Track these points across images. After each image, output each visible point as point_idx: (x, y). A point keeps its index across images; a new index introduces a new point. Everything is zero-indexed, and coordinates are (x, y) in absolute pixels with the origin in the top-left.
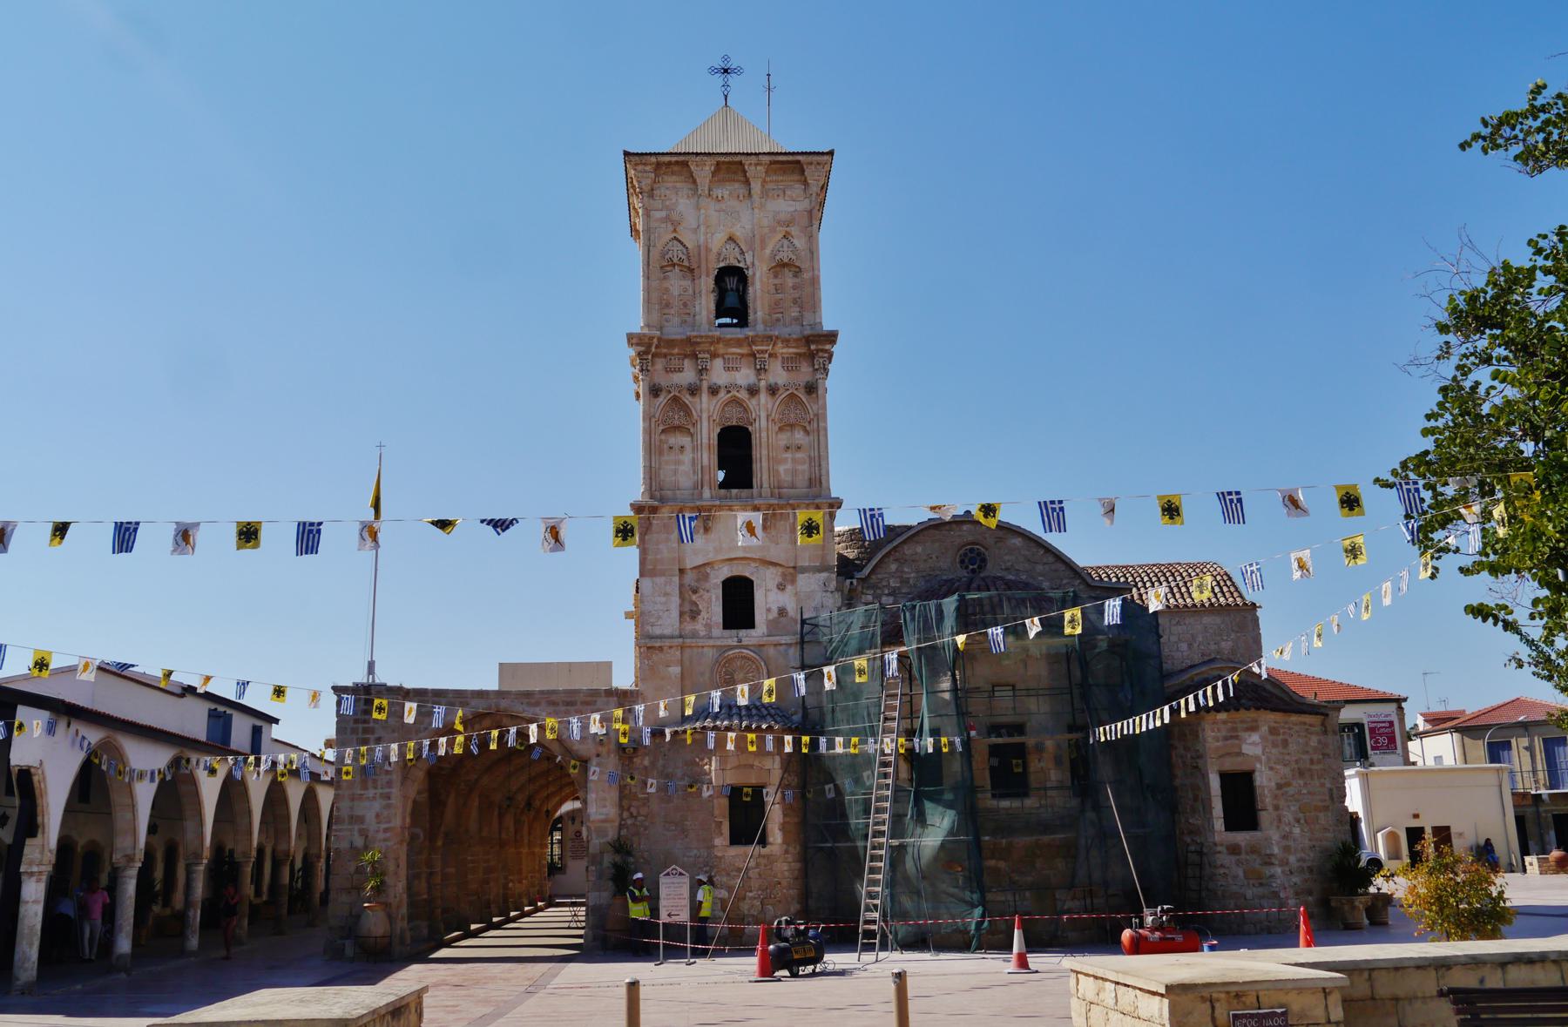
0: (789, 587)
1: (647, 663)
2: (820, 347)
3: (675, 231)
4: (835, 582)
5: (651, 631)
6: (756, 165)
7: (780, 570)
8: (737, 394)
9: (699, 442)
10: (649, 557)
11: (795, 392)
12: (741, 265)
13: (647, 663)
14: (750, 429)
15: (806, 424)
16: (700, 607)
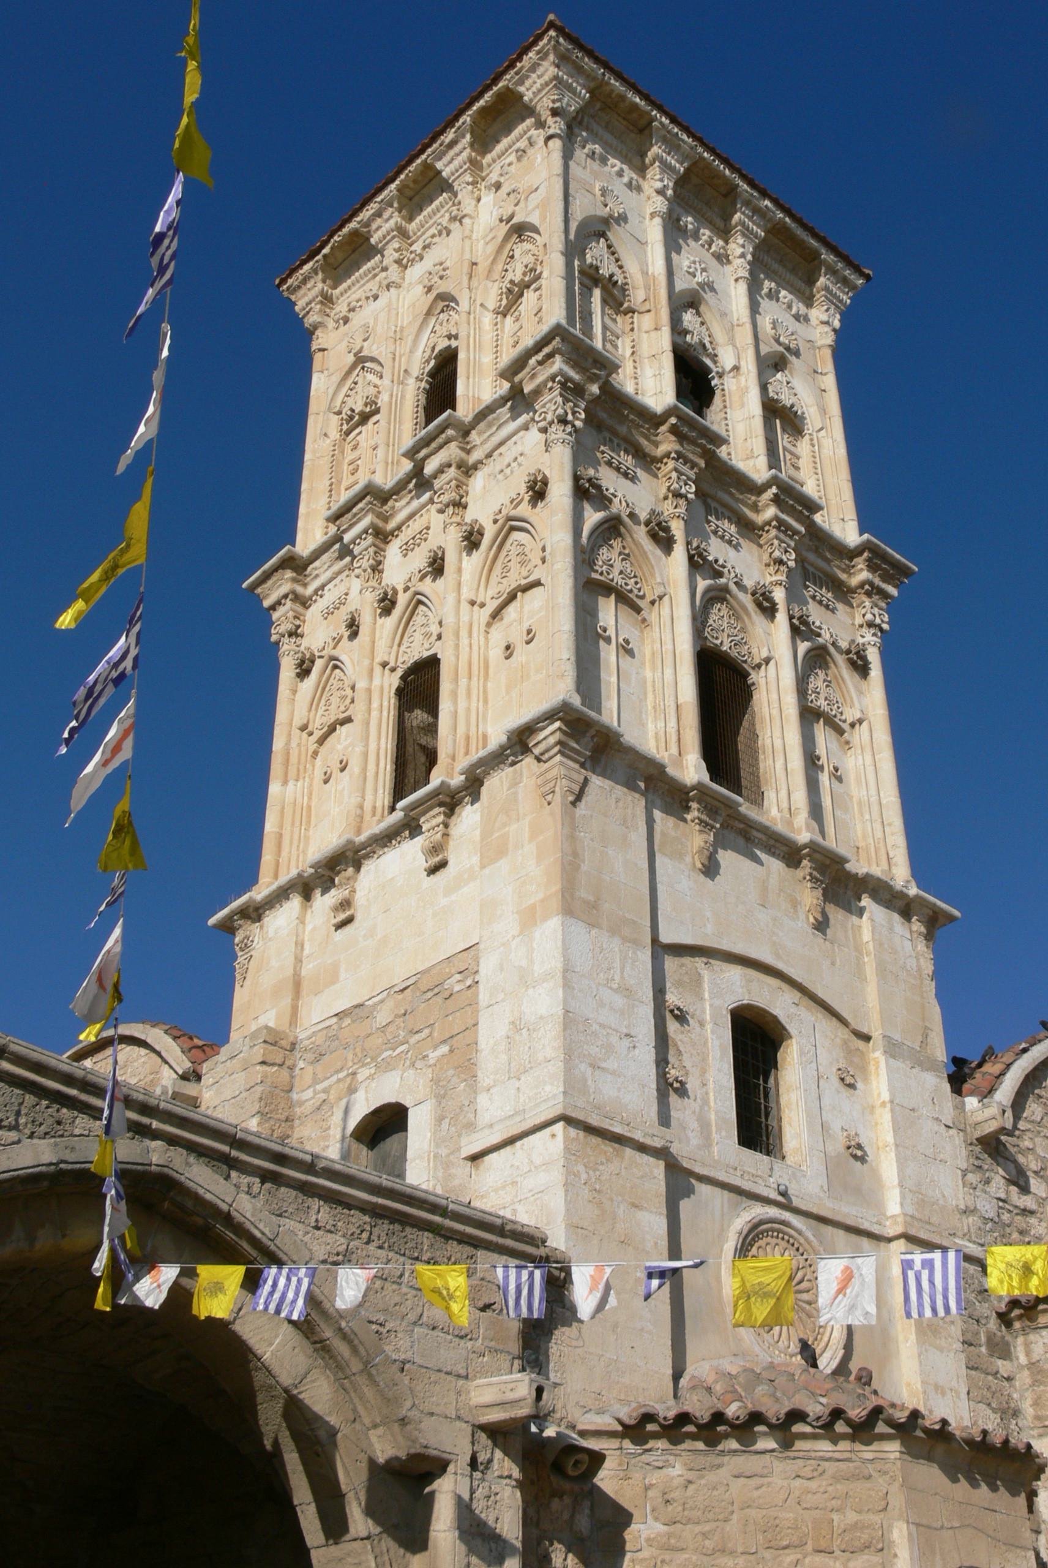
0: (860, 1085)
1: (584, 1176)
2: (884, 586)
3: (606, 221)
4: (950, 1104)
5: (589, 1082)
6: (757, 211)
7: (843, 1033)
8: (733, 587)
9: (668, 646)
10: (584, 868)
11: (832, 649)
12: (708, 362)
13: (584, 1176)
14: (753, 677)
15: (846, 726)
16: (688, 1064)
